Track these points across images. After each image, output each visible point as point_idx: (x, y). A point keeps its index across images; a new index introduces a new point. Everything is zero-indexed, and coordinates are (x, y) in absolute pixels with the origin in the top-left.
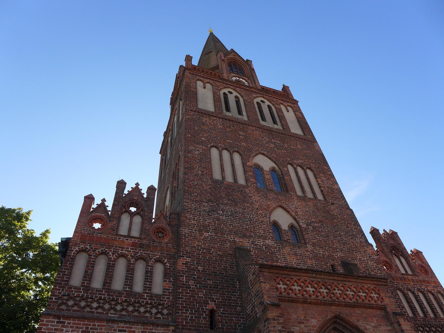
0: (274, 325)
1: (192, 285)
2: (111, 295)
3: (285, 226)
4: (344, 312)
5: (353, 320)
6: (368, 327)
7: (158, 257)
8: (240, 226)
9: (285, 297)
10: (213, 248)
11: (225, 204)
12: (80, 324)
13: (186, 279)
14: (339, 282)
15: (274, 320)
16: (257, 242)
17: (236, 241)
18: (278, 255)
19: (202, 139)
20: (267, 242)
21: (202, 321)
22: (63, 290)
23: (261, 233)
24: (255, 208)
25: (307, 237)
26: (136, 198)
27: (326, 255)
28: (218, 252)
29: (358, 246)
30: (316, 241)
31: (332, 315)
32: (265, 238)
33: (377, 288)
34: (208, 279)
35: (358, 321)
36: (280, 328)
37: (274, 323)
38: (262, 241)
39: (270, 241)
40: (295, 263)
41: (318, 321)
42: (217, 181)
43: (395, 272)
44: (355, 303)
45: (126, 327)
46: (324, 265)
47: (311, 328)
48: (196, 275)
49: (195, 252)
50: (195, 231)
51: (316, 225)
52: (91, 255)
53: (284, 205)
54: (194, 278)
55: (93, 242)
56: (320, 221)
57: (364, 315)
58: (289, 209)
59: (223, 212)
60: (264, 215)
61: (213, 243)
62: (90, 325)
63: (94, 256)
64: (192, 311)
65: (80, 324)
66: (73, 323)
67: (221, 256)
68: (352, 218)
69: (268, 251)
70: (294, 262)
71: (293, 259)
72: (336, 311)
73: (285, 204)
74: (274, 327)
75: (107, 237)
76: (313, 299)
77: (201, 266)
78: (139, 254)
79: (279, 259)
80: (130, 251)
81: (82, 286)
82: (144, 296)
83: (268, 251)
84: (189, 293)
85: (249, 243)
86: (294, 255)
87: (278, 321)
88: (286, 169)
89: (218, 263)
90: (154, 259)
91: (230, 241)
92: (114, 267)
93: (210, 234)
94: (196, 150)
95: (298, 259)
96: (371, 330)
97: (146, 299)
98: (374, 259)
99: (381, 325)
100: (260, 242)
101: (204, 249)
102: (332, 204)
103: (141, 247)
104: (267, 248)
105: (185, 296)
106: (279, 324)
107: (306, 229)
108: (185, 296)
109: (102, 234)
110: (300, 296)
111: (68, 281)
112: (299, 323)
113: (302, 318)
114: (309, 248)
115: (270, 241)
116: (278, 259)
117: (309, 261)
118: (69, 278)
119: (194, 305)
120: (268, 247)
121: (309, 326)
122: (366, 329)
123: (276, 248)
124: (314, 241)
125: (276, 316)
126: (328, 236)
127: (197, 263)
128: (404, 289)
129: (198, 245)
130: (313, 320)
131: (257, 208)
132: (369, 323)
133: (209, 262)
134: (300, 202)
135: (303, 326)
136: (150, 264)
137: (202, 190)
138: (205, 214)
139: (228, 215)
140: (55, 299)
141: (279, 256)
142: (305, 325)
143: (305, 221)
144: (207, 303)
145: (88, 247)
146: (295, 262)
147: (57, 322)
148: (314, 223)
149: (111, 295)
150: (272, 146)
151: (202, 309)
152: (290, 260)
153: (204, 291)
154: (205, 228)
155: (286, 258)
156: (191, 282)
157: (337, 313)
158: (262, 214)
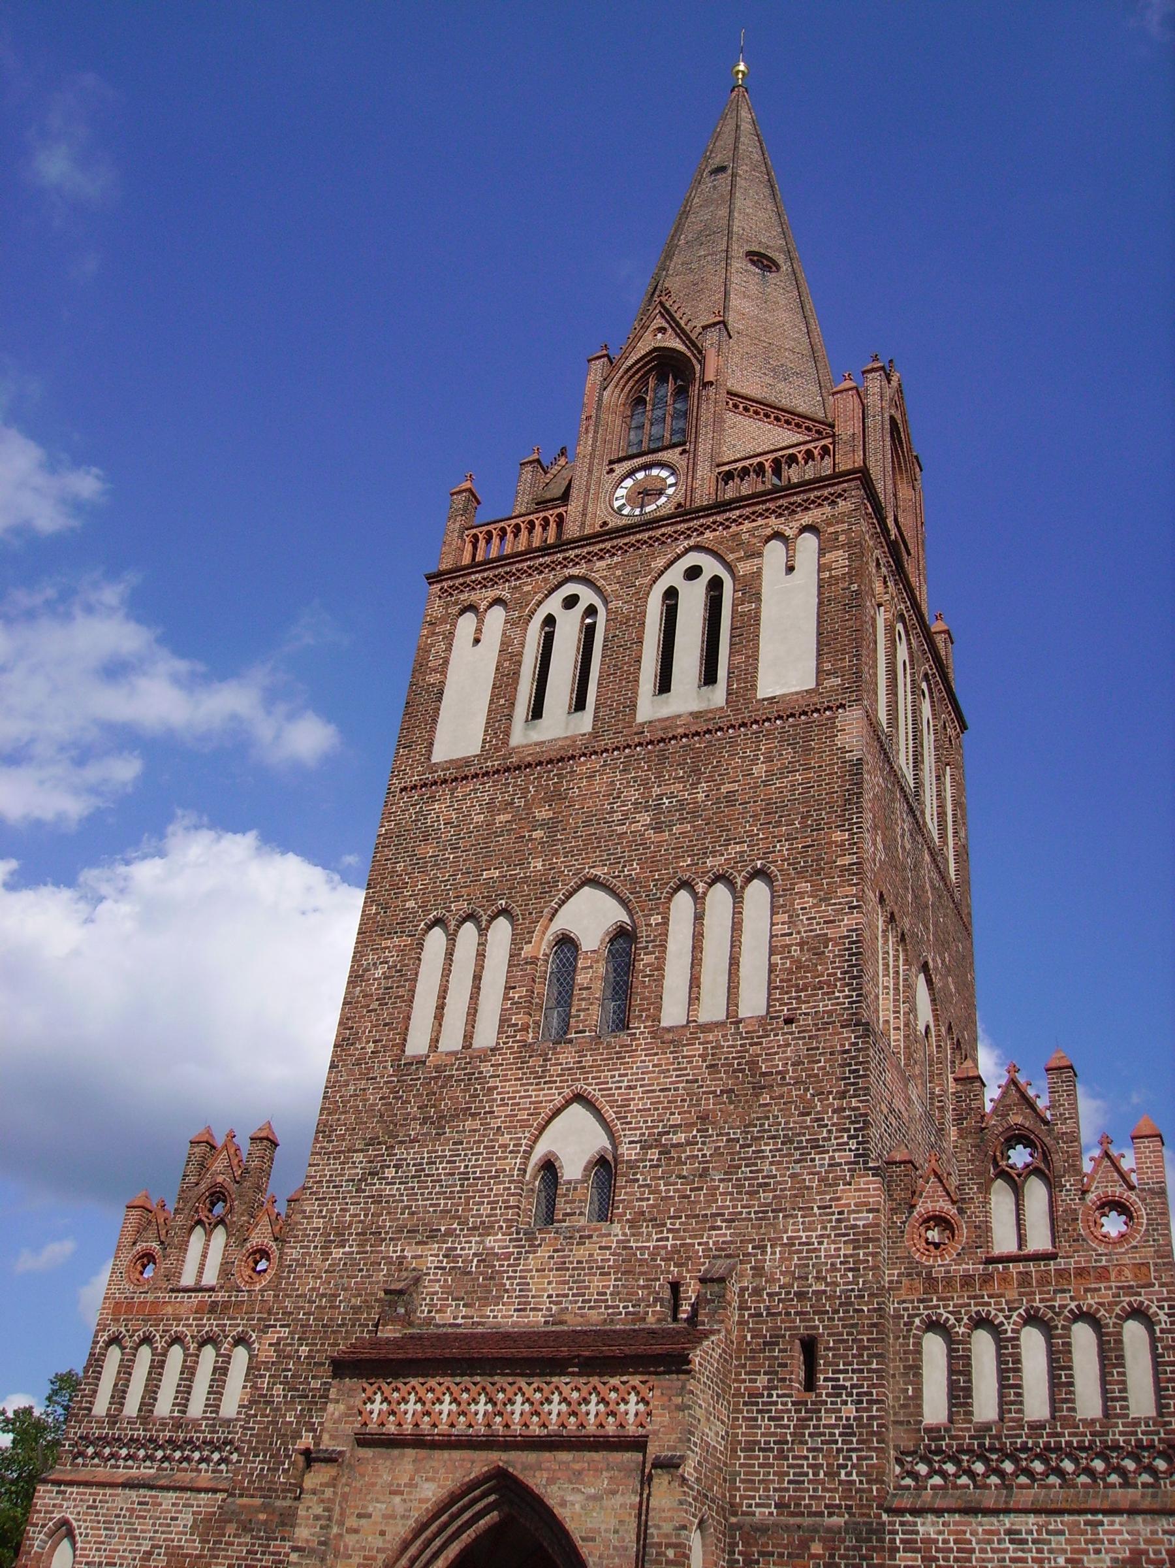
0: (311, 1505)
1: (278, 1396)
2: (150, 1430)
3: (572, 1169)
4: (517, 1462)
5: (536, 1482)
6: (570, 1498)
7: (240, 1329)
8: (431, 1205)
9: (372, 1434)
10: (344, 1289)
11: (412, 1141)
12: (85, 1494)
13: (268, 1384)
14: (532, 1380)
15: (314, 1492)
16: (462, 1249)
17: (405, 1257)
18: (508, 1278)
19: (408, 905)
20: (490, 1241)
21: (279, 1478)
22: (80, 1428)
23: (481, 1216)
24: (492, 1129)
25: (626, 1193)
26: (220, 1179)
27: (663, 1252)
28: (353, 1300)
29: (809, 1188)
30: (651, 1202)
31: (486, 1469)
32: (485, 1229)
33: (650, 1384)
34: (314, 1377)
35: (551, 1481)
36: (319, 1510)
37: (311, 1499)
38: (476, 1242)
39: (500, 1236)
40: (550, 1296)
41: (439, 1487)
42: (406, 1067)
43: (959, 1254)
44: (552, 1436)
45: (150, 1497)
46: (643, 1287)
47: (416, 1504)
48: (290, 1370)
49: (303, 1308)
50: (316, 1247)
51: (681, 1137)
52: (125, 1348)
53: (589, 1089)
54: (286, 1377)
55: (131, 1317)
56: (703, 1118)
57: (577, 1466)
58: (602, 1103)
59: (397, 1172)
60: (511, 1148)
61: (348, 1277)
62: (98, 1494)
63: (131, 1348)
64: (265, 1456)
65: (85, 1494)
66: (77, 1493)
67: (356, 1310)
68: (841, 1066)
69: (481, 1273)
70: (546, 1295)
71: (549, 1283)
72: (500, 1460)
73: (597, 1084)
74: (309, 1508)
75: (156, 1298)
76: (437, 1435)
77: (307, 1345)
78: (207, 1329)
79: (507, 1291)
80: (191, 1325)
81: (107, 1415)
82: (201, 1425)
83: (481, 1273)
84: (267, 1416)
85: (437, 1256)
86: (557, 1269)
87: (322, 1496)
88: (656, 919)
89: (346, 1332)
90: (233, 1337)
91: (390, 1262)
92: (162, 1368)
93: (347, 1249)
94: (381, 963)
95: (566, 1282)
96: (577, 1506)
97: (204, 1432)
98: (854, 1227)
99: (614, 1493)
100: (469, 1247)
101: (324, 1295)
102: (789, 1021)
103: (210, 1312)
104: (484, 1261)
105: (259, 1423)
106: (322, 1501)
107: (631, 1165)
108: (259, 1423)
109: (147, 1293)
110: (407, 1430)
111: (90, 1410)
112: (392, 1493)
113: (405, 1479)
114: (616, 1235)
115: (500, 1236)
116: (502, 1294)
117: (597, 1283)
118: (91, 1403)
119: (271, 1444)
120: (485, 1258)
121: (411, 1501)
122: (563, 1504)
123: (508, 1256)
124: (644, 1204)
125: (321, 1485)
126: (704, 1173)
127: (299, 1339)
128: (959, 1320)
129: (313, 1289)
130: (426, 1485)
131: (499, 1128)
132: (581, 1487)
133: (325, 1332)
134: (656, 1054)
135: (397, 1499)
136: (222, 1351)
137: (360, 1112)
138: (350, 1192)
139: (407, 1177)
140: (69, 1446)
141: (508, 1282)
142: (405, 1497)
143: (644, 1134)
144: (297, 1435)
145: (123, 1329)
146: (551, 1292)
147: (57, 1492)
148: (675, 1133)
149: (150, 1430)
150: (646, 818)
151: (286, 1449)
152: (537, 1290)
153: (299, 1408)
154: (339, 1235)
155: (528, 1284)
156: (279, 1389)
157: (501, 1464)
158: (505, 1146)
